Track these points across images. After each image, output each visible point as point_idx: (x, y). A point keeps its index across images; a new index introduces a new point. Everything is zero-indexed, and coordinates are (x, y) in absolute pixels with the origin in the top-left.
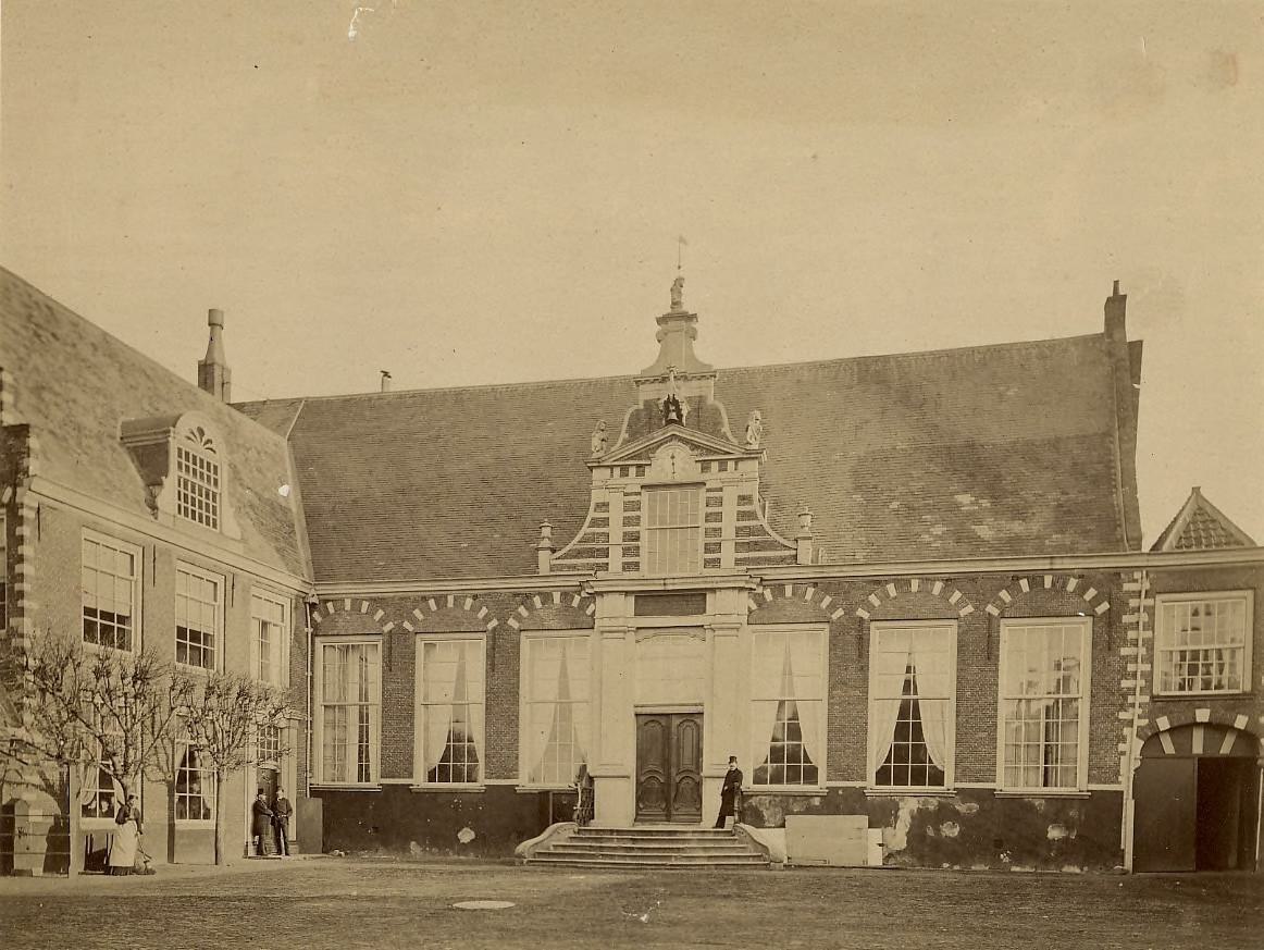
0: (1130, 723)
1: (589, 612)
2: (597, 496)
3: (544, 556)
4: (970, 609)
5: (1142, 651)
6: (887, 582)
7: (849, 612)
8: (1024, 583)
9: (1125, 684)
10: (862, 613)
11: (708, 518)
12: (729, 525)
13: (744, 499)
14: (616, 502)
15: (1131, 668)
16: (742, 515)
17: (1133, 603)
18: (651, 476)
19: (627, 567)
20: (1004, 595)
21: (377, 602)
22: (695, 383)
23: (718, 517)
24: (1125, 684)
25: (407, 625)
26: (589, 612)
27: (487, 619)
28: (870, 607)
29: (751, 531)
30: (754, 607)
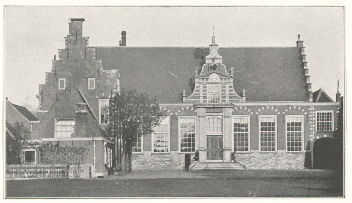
0: (312, 137)
1: (195, 111)
2: (196, 85)
3: (184, 98)
4: (279, 113)
5: (314, 122)
6: (262, 106)
7: (281, 113)
8: (290, 108)
9: (311, 129)
10: (257, 113)
11: (222, 90)
12: (227, 93)
13: (230, 87)
14: (201, 86)
15: (311, 126)
16: (230, 91)
17: (311, 112)
18: (209, 81)
19: (223, 101)
20: (286, 110)
21: (275, 107)
22: (218, 60)
23: (225, 90)
24: (311, 129)
26: (195, 111)
27: (170, 113)
28: (259, 112)
29: (232, 94)
30: (233, 111)
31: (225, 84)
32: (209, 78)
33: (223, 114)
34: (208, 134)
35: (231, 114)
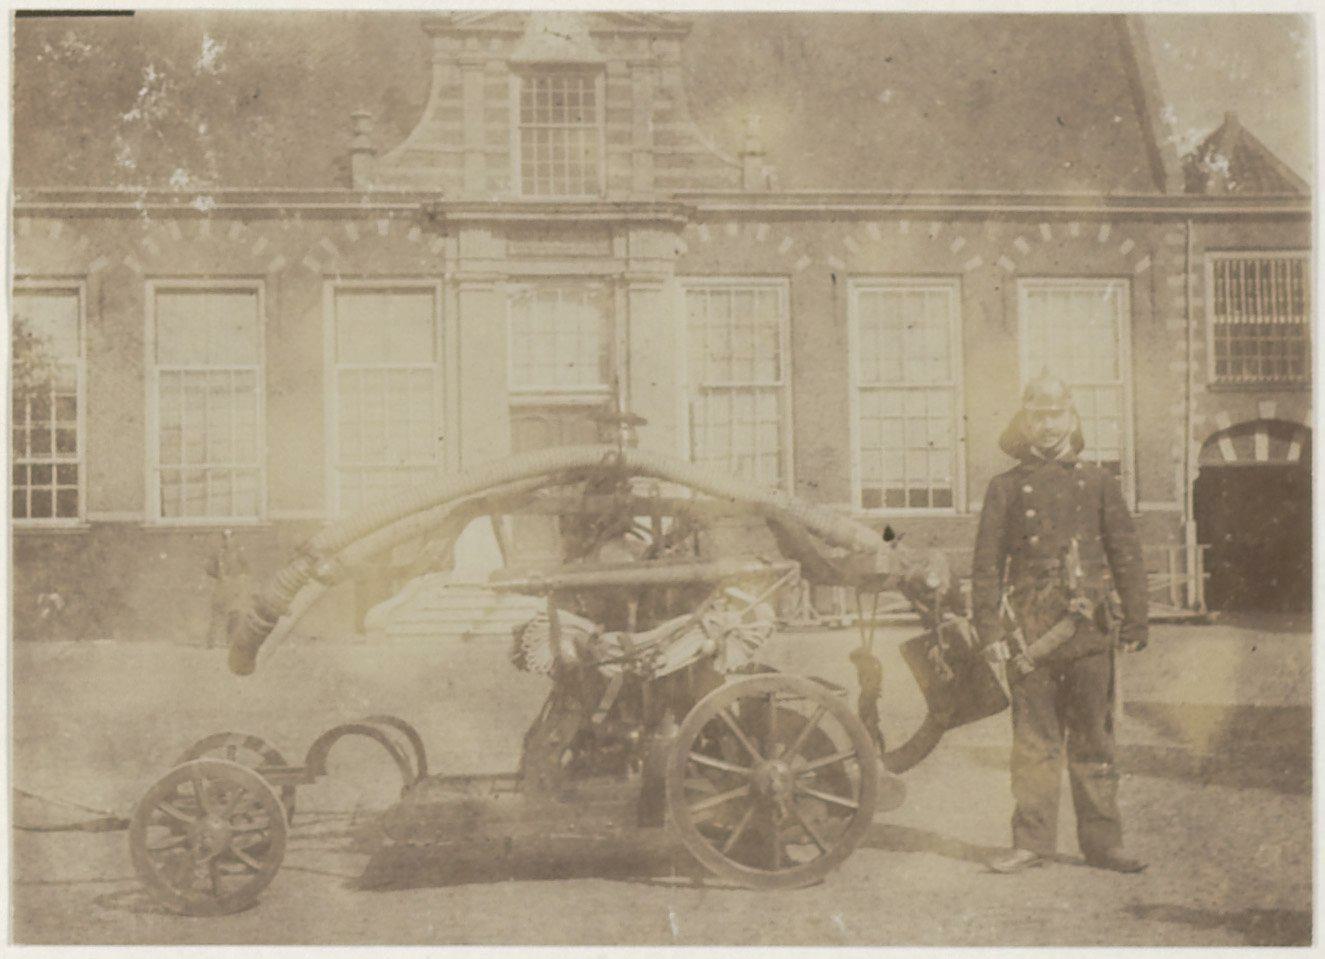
2: (441, 74)
13: (664, 93)
20: (1021, 244)
25: (129, 261)
26: (435, 250)
31: (629, 76)
32: (522, 33)
33: (613, 268)
34: (517, 401)
35: (670, 268)
